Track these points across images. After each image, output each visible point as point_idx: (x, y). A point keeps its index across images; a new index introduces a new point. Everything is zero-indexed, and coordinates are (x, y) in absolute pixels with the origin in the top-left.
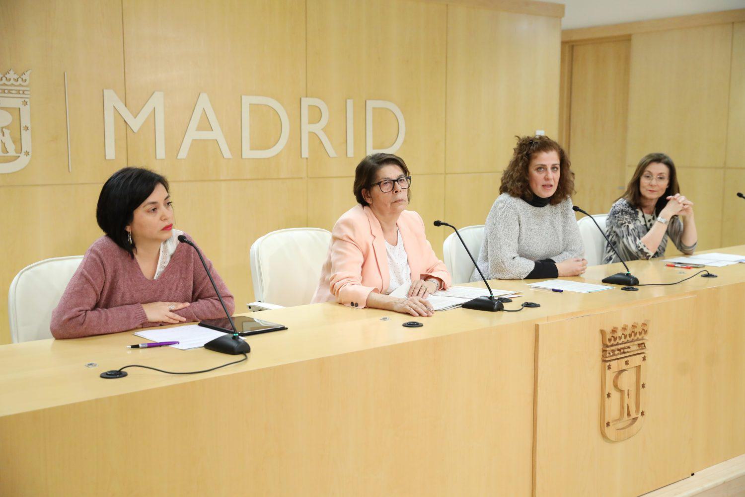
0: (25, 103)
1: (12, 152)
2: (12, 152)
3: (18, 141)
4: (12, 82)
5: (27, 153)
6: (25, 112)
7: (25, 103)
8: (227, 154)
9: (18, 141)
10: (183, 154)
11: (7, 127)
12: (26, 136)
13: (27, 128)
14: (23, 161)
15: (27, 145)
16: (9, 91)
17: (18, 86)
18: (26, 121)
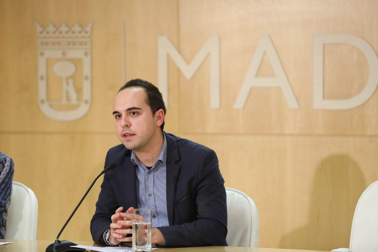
0: (86, 54)
1: (74, 100)
2: (74, 100)
3: (79, 91)
4: (76, 34)
5: (86, 102)
6: (87, 61)
7: (86, 54)
8: (292, 103)
9: (79, 91)
10: (239, 104)
11: (72, 77)
12: (86, 85)
13: (86, 78)
14: (83, 109)
15: (86, 94)
16: (74, 43)
17: (83, 37)
18: (87, 71)
